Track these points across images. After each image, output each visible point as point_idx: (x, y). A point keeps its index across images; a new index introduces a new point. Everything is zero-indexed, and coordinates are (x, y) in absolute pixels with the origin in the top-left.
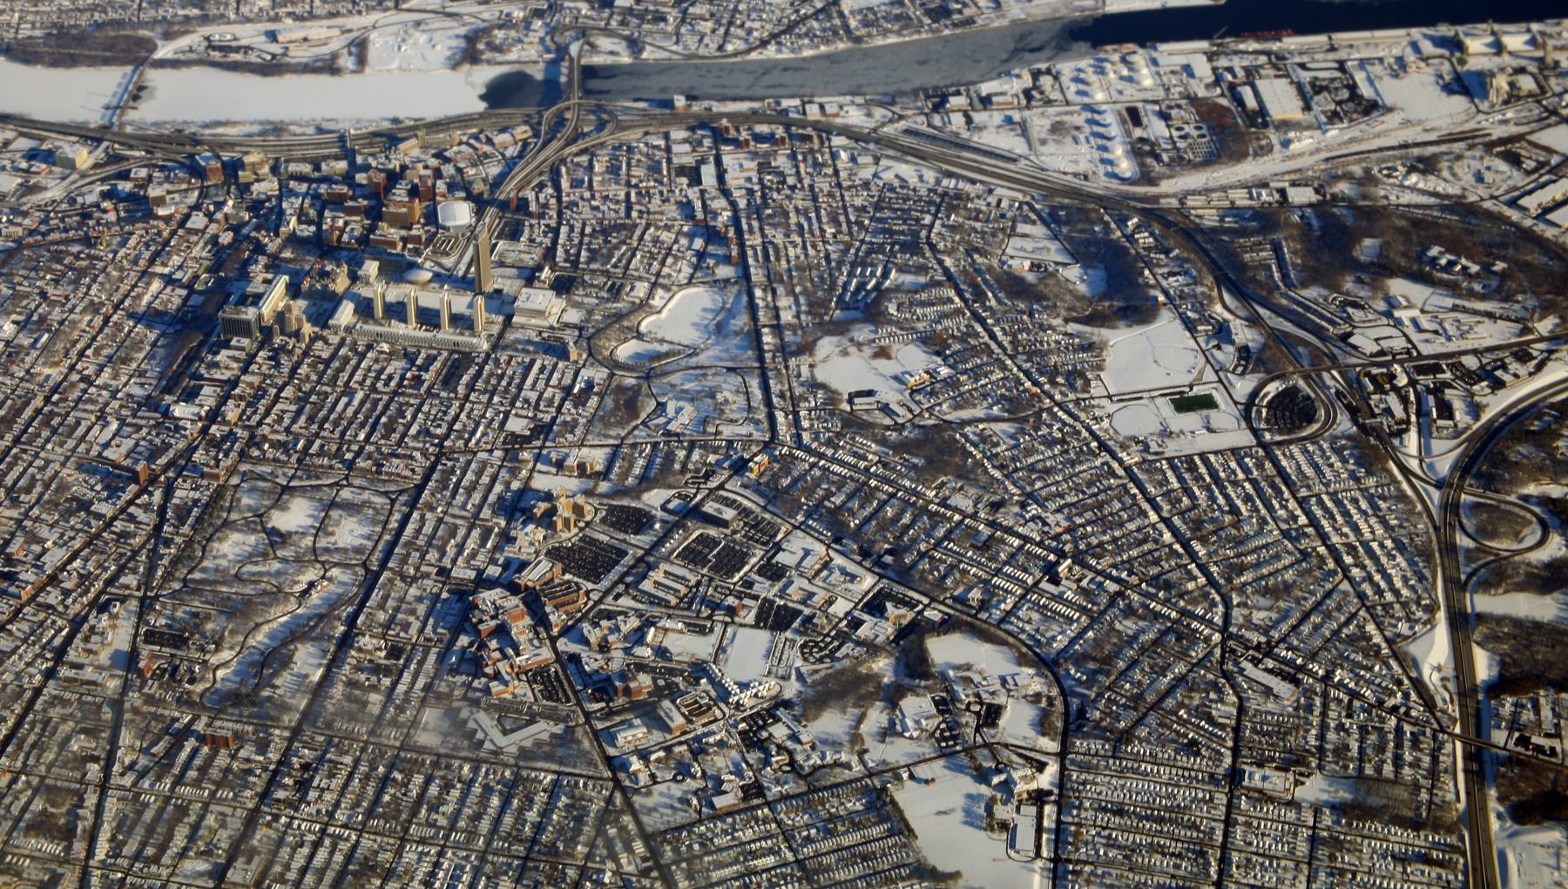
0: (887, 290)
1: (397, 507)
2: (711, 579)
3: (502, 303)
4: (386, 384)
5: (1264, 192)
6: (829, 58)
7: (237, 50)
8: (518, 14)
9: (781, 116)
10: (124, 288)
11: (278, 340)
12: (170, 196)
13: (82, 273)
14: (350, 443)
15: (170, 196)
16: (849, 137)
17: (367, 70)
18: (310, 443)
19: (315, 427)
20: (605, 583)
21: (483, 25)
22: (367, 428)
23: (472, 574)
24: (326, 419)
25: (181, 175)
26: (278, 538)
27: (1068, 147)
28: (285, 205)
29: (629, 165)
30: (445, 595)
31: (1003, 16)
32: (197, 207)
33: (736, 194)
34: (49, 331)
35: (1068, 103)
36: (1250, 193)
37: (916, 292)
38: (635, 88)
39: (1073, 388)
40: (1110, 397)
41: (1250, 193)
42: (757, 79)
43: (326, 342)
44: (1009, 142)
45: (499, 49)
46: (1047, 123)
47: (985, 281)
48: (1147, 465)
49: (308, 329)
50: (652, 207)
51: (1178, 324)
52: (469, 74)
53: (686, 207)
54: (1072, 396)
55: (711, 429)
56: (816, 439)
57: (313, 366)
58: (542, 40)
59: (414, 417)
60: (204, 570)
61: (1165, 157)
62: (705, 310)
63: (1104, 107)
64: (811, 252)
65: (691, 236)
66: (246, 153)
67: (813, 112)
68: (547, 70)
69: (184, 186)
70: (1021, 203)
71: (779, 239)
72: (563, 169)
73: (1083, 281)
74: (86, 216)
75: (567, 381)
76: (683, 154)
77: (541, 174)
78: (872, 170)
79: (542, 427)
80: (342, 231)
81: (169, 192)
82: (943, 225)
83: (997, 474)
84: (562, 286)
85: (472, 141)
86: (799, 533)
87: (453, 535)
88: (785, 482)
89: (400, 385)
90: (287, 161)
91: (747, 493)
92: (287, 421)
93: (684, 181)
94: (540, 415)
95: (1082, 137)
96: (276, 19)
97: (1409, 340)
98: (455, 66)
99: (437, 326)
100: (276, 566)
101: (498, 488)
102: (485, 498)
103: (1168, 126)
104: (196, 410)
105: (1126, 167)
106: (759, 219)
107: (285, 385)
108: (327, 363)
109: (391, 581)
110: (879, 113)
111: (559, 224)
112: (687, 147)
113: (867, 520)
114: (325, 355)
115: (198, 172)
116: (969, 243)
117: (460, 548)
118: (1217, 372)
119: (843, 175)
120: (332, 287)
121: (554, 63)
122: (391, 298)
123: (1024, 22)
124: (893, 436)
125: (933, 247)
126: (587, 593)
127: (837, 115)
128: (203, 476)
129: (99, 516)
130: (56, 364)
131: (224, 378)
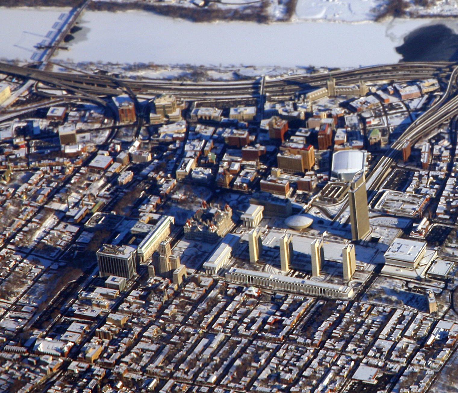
3: (373, 251)
4: (248, 328)
10: (19, 222)
11: (152, 280)
12: (81, 136)
14: (201, 384)
15: (81, 136)
17: (294, 19)
18: (162, 382)
19: (171, 367)
22: (221, 371)
24: (183, 360)
25: (95, 115)
28: (187, 148)
32: (104, 147)
49: (181, 270)
52: (391, 26)
57: (181, 307)
59: (268, 361)
66: (159, 96)
69: (97, 126)
75: (423, 332)
77: (440, 126)
79: (390, 377)
80: (237, 174)
81: (80, 131)
85: (380, 92)
90: (199, 105)
92: (145, 360)
94: (390, 365)
98: (378, 17)
99: (309, 273)
104: (59, 345)
107: (151, 323)
108: (195, 304)
111: (448, 176)
115: (111, 112)
120: (213, 229)
122: (269, 242)
131: (94, 315)
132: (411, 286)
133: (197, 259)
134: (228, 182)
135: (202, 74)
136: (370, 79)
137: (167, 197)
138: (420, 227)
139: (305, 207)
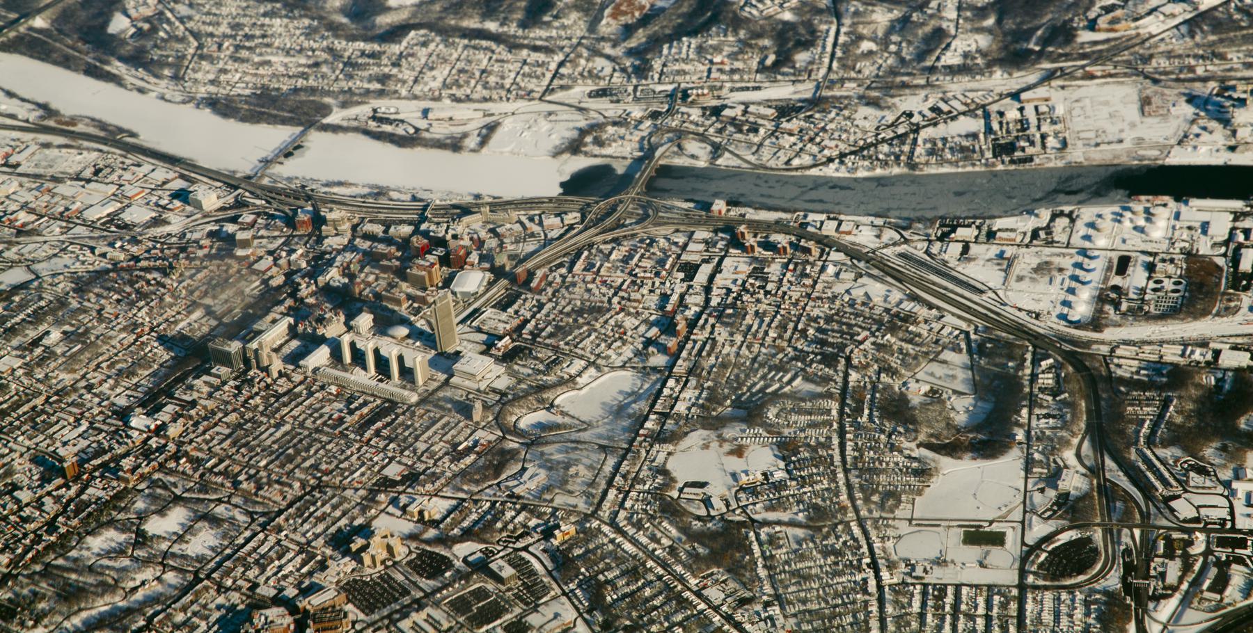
0: (786, 396)
1: (253, 527)
2: (462, 626)
3: (446, 361)
4: (314, 422)
5: (1198, 351)
6: (880, 181)
7: (388, 121)
8: (637, 112)
9: (801, 230)
10: (170, 312)
13: (142, 295)
14: (253, 466)
16: (846, 254)
17: (485, 150)
18: (221, 461)
19: (234, 450)
20: (376, 617)
21: (601, 119)
22: (273, 457)
23: (273, 592)
25: (279, 223)
26: (142, 539)
27: (1042, 285)
29: (642, 256)
30: (241, 607)
31: (1062, 158)
32: (270, 253)
33: (715, 291)
34: (83, 343)
36: (1184, 352)
37: (803, 400)
39: (882, 506)
40: (910, 521)
42: (803, 193)
43: (289, 379)
45: (599, 142)
46: (1035, 262)
47: (873, 397)
48: (900, 589)
49: (277, 365)
50: (634, 296)
51: (1020, 463)
52: (566, 162)
53: (665, 297)
54: (876, 514)
55: (548, 497)
56: (629, 519)
58: (643, 138)
59: (316, 452)
60: (67, 559)
61: (1124, 307)
62: (621, 392)
63: (1096, 253)
64: (744, 351)
65: (651, 325)
66: (331, 210)
67: (829, 228)
68: (630, 167)
69: (276, 233)
70: (962, 331)
71: (720, 339)
72: (586, 253)
73: (967, 411)
74: (183, 249)
77: (564, 256)
82: (873, 343)
83: (763, 573)
84: (508, 357)
86: (564, 599)
87: (279, 559)
88: (578, 552)
89: (324, 424)
91: (544, 557)
93: (681, 275)
95: (1059, 278)
96: (438, 99)
97: (1232, 513)
98: (557, 153)
99: (389, 377)
101: (344, 522)
102: (328, 528)
103: (1149, 278)
105: (1082, 308)
106: (719, 318)
107: (234, 410)
109: (206, 589)
110: (889, 235)
112: (702, 247)
113: (625, 596)
114: (280, 391)
115: (290, 222)
116: (885, 361)
117: (280, 568)
118: (1025, 512)
119: (819, 287)
121: (639, 161)
123: (1079, 166)
124: (697, 525)
125: (848, 359)
126: (354, 623)
127: (849, 233)
128: (118, 479)
129: (18, 501)
130: (74, 371)
132: (471, 396)
133: (295, 359)
134: (357, 291)
135: (384, 194)
136: (524, 209)
137: (302, 299)
138: (500, 344)
139: (412, 318)
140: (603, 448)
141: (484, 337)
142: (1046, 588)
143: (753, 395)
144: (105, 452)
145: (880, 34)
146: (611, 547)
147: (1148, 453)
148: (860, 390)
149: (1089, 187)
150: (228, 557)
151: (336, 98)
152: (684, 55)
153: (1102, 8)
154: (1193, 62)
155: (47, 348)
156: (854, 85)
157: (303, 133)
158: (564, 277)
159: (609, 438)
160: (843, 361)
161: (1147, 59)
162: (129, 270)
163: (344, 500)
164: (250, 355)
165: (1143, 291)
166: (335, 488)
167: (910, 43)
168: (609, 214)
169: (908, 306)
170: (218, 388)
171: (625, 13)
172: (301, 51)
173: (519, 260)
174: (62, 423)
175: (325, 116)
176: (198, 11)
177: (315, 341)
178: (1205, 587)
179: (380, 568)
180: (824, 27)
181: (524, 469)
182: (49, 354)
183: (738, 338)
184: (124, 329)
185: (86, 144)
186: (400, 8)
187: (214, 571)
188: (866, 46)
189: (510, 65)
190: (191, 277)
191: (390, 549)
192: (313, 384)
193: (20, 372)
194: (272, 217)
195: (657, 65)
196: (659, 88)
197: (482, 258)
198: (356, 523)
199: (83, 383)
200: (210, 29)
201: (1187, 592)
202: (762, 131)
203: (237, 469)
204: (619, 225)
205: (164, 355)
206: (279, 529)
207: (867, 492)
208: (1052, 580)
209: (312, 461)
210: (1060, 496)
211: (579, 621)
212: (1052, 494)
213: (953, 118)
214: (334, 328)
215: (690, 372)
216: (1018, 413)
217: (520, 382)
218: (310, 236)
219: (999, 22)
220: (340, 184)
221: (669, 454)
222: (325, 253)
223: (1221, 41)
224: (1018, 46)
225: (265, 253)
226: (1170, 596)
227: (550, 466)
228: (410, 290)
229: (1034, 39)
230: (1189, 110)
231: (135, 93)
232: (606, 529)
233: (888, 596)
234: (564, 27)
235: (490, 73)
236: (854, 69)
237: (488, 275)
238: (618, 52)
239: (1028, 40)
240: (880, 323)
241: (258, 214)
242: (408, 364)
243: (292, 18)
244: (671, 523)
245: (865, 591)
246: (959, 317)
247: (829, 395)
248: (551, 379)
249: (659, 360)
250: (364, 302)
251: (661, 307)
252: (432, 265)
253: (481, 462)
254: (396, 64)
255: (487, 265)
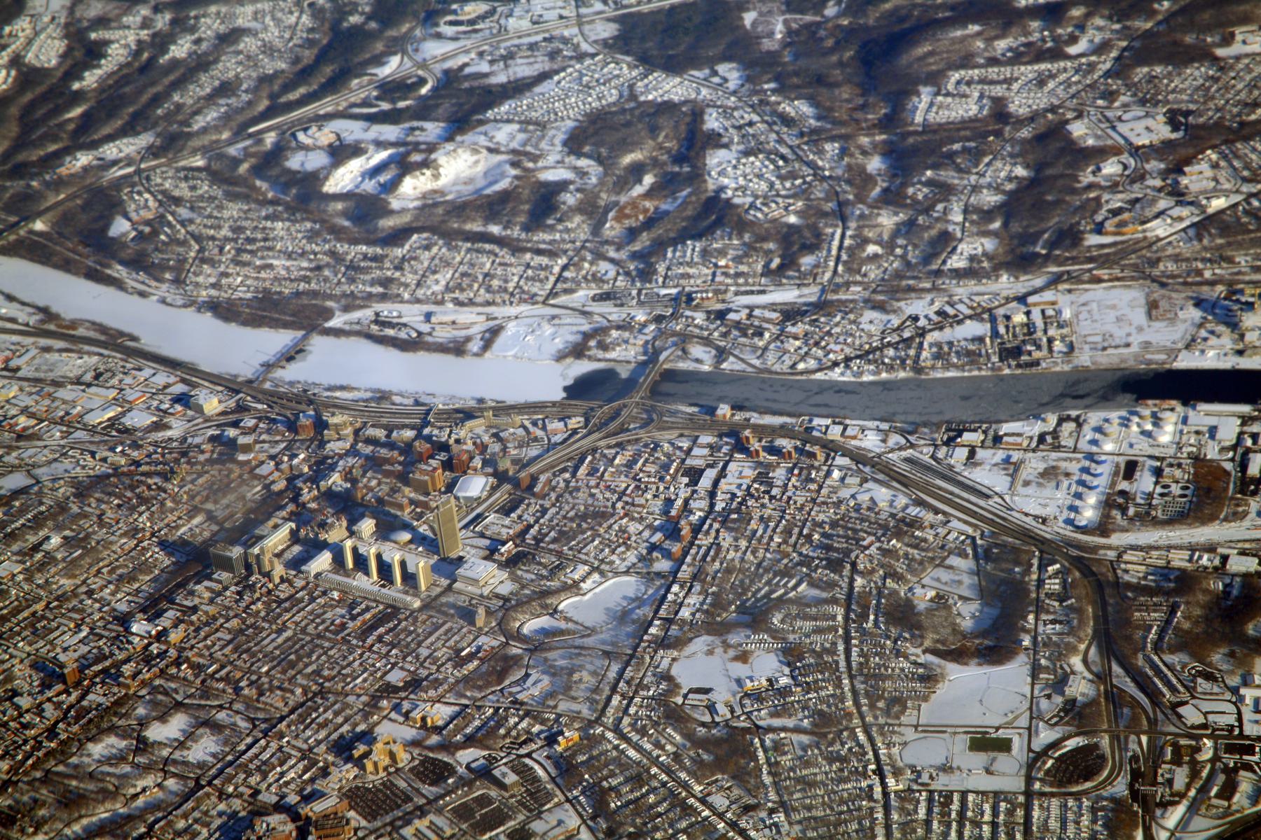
0: (791, 601)
3: (449, 566)
5: (1206, 557)
6: (885, 385)
7: (391, 325)
8: (641, 317)
10: (171, 517)
13: (143, 500)
14: (254, 673)
17: (488, 355)
18: (222, 667)
20: (378, 823)
23: (274, 799)
24: (246, 651)
25: (280, 427)
26: (143, 745)
27: (1049, 491)
29: (646, 461)
30: (243, 814)
31: (1069, 362)
32: (272, 457)
33: (720, 496)
34: (84, 548)
35: (1075, 450)
36: (1191, 557)
37: (809, 606)
38: (699, 394)
39: (887, 712)
40: (916, 727)
41: (1191, 557)
43: (291, 584)
44: (996, 481)
45: (603, 346)
46: (1041, 467)
47: (879, 602)
48: (906, 796)
49: (279, 570)
50: (638, 501)
51: (1026, 670)
52: (569, 366)
54: (881, 721)
55: (551, 703)
58: (647, 342)
60: (67, 765)
61: (1131, 512)
62: (625, 598)
63: (1103, 458)
64: (749, 556)
65: (655, 530)
66: (333, 414)
67: (835, 432)
68: (634, 371)
70: (968, 536)
71: (725, 545)
73: (973, 617)
74: (184, 454)
76: (699, 457)
78: (853, 491)
83: (767, 780)
84: (511, 563)
86: (567, 806)
87: (281, 765)
88: (581, 758)
89: (326, 629)
93: (686, 480)
95: (1066, 483)
96: (441, 303)
97: (1240, 719)
98: (560, 357)
100: (127, 769)
101: (346, 728)
103: (1156, 483)
105: (1089, 514)
106: (723, 523)
109: (208, 795)
110: (895, 439)
112: (706, 451)
114: (282, 596)
115: (292, 426)
116: (891, 566)
118: (1031, 718)
119: (824, 491)
121: (643, 364)
124: (702, 731)
125: (854, 565)
126: (356, 830)
128: (119, 685)
129: (18, 707)
130: (74, 576)
133: (297, 564)
137: (304, 505)
140: (607, 654)
141: (487, 542)
142: (1053, 795)
143: (758, 600)
144: (106, 658)
145: (886, 237)
146: (615, 753)
147: (1156, 658)
148: (865, 595)
149: (1096, 391)
150: (229, 764)
151: (338, 301)
152: (688, 259)
153: (1109, 211)
154: (1200, 265)
155: (47, 553)
156: (859, 289)
157: (305, 337)
158: (567, 482)
159: (613, 644)
160: (848, 566)
161: (1154, 263)
162: (129, 474)
163: (347, 706)
164: (252, 560)
165: (1150, 496)
166: (337, 694)
167: (915, 246)
168: (613, 418)
169: (914, 511)
170: (219, 594)
171: (628, 217)
172: (303, 254)
173: (522, 464)
174: (63, 628)
175: (328, 319)
176: (200, 214)
177: (317, 546)
178: (1213, 793)
179: (382, 774)
180: (830, 230)
181: (527, 675)
182: (50, 559)
183: (743, 543)
184: (124, 535)
185: (86, 348)
186: (403, 211)
187: (215, 777)
188: (872, 249)
189: (514, 270)
190: (192, 482)
191: (392, 755)
192: (316, 588)
193: (21, 577)
194: (274, 421)
195: (661, 268)
196: (663, 292)
197: (485, 463)
198: (359, 729)
199: (84, 589)
200: (212, 232)
201: (1195, 799)
202: (767, 335)
203: (238, 675)
204: (622, 430)
205: (165, 561)
206: (281, 736)
207: (873, 699)
208: (1059, 786)
209: (314, 667)
210: (1066, 702)
211: (583, 828)
212: (1059, 700)
213: (960, 322)
214: (336, 533)
215: (695, 577)
216: (1025, 618)
217: (523, 587)
218: (312, 441)
219: (1005, 225)
220: (342, 388)
221: (674, 660)
222: (327, 457)
223: (1229, 244)
224: (1024, 250)
225: (267, 458)
226: (1177, 803)
227: (553, 672)
228: (412, 495)
229: (1041, 243)
230: (1195, 314)
231: (136, 297)
232: (609, 735)
233: (894, 803)
234: (568, 230)
235: (493, 277)
236: (859, 272)
237: (491, 479)
238: (622, 255)
239: (1034, 243)
240: (885, 528)
241: (260, 419)
242: (411, 569)
243: (294, 222)
244: (675, 729)
245: (870, 798)
246: (966, 522)
247: (834, 601)
248: (554, 584)
249: (663, 565)
250: (366, 507)
251: (666, 512)
252: (435, 469)
253: (484, 668)
254: (399, 268)
255: (490, 470)
